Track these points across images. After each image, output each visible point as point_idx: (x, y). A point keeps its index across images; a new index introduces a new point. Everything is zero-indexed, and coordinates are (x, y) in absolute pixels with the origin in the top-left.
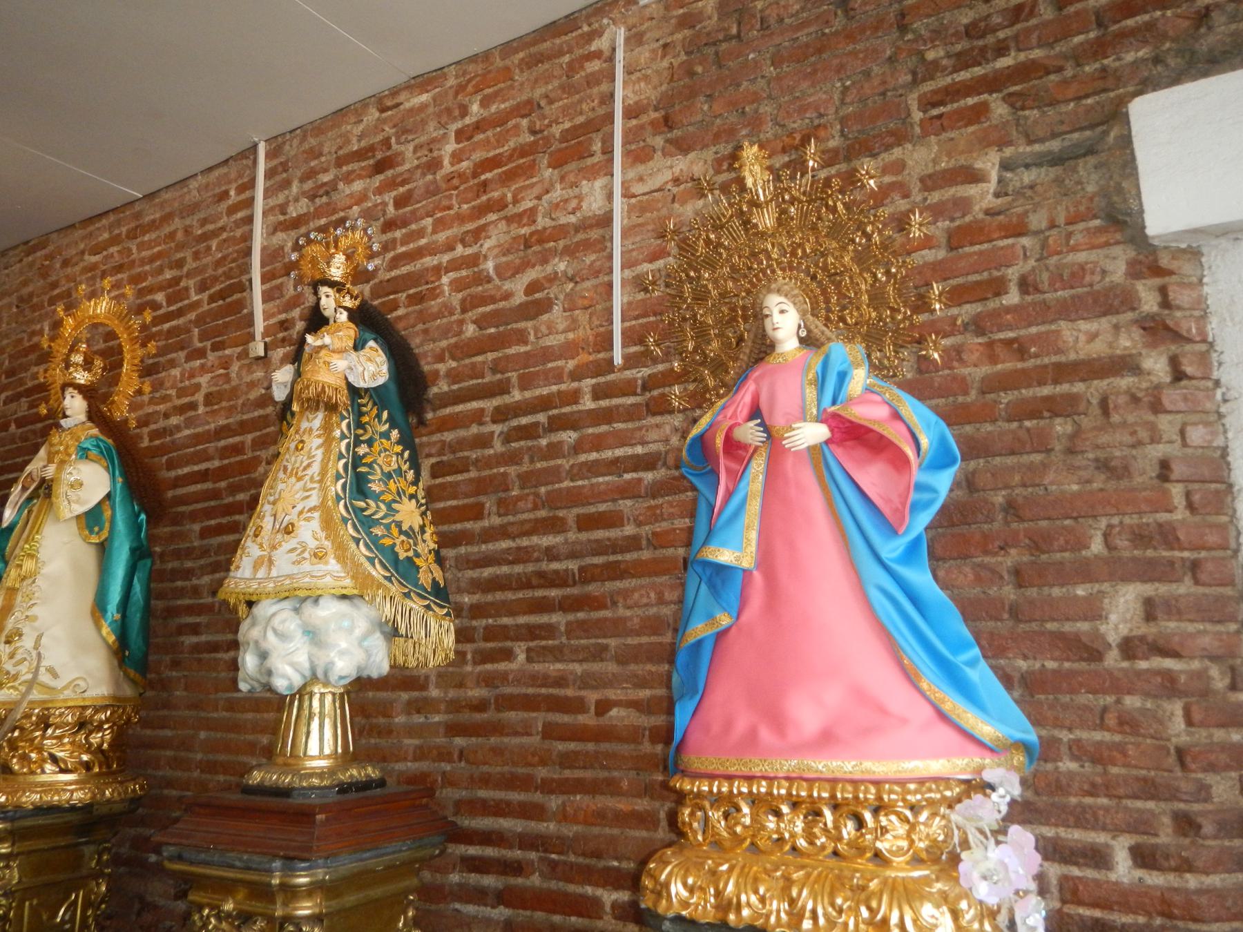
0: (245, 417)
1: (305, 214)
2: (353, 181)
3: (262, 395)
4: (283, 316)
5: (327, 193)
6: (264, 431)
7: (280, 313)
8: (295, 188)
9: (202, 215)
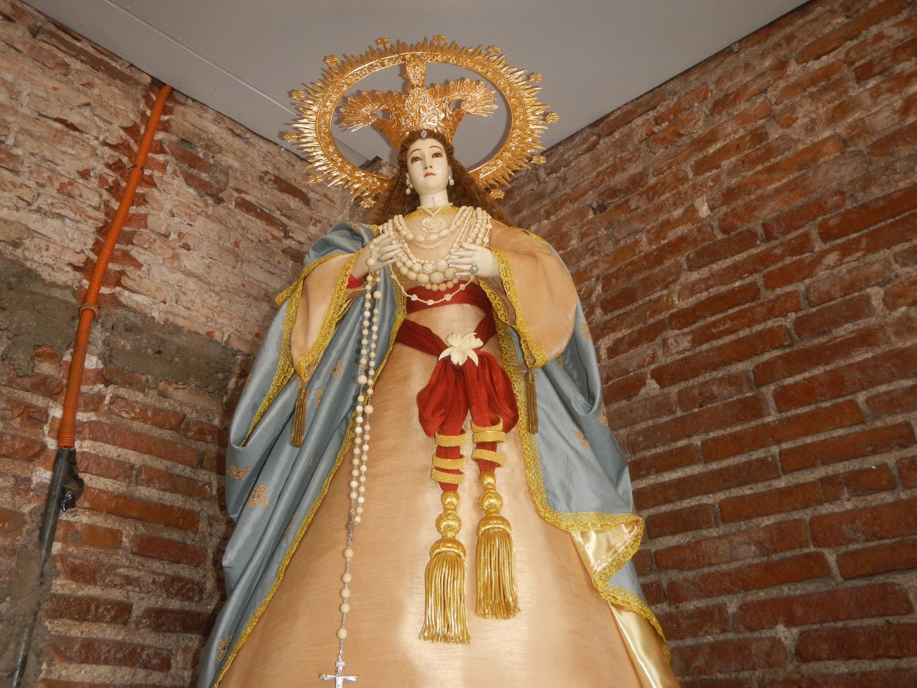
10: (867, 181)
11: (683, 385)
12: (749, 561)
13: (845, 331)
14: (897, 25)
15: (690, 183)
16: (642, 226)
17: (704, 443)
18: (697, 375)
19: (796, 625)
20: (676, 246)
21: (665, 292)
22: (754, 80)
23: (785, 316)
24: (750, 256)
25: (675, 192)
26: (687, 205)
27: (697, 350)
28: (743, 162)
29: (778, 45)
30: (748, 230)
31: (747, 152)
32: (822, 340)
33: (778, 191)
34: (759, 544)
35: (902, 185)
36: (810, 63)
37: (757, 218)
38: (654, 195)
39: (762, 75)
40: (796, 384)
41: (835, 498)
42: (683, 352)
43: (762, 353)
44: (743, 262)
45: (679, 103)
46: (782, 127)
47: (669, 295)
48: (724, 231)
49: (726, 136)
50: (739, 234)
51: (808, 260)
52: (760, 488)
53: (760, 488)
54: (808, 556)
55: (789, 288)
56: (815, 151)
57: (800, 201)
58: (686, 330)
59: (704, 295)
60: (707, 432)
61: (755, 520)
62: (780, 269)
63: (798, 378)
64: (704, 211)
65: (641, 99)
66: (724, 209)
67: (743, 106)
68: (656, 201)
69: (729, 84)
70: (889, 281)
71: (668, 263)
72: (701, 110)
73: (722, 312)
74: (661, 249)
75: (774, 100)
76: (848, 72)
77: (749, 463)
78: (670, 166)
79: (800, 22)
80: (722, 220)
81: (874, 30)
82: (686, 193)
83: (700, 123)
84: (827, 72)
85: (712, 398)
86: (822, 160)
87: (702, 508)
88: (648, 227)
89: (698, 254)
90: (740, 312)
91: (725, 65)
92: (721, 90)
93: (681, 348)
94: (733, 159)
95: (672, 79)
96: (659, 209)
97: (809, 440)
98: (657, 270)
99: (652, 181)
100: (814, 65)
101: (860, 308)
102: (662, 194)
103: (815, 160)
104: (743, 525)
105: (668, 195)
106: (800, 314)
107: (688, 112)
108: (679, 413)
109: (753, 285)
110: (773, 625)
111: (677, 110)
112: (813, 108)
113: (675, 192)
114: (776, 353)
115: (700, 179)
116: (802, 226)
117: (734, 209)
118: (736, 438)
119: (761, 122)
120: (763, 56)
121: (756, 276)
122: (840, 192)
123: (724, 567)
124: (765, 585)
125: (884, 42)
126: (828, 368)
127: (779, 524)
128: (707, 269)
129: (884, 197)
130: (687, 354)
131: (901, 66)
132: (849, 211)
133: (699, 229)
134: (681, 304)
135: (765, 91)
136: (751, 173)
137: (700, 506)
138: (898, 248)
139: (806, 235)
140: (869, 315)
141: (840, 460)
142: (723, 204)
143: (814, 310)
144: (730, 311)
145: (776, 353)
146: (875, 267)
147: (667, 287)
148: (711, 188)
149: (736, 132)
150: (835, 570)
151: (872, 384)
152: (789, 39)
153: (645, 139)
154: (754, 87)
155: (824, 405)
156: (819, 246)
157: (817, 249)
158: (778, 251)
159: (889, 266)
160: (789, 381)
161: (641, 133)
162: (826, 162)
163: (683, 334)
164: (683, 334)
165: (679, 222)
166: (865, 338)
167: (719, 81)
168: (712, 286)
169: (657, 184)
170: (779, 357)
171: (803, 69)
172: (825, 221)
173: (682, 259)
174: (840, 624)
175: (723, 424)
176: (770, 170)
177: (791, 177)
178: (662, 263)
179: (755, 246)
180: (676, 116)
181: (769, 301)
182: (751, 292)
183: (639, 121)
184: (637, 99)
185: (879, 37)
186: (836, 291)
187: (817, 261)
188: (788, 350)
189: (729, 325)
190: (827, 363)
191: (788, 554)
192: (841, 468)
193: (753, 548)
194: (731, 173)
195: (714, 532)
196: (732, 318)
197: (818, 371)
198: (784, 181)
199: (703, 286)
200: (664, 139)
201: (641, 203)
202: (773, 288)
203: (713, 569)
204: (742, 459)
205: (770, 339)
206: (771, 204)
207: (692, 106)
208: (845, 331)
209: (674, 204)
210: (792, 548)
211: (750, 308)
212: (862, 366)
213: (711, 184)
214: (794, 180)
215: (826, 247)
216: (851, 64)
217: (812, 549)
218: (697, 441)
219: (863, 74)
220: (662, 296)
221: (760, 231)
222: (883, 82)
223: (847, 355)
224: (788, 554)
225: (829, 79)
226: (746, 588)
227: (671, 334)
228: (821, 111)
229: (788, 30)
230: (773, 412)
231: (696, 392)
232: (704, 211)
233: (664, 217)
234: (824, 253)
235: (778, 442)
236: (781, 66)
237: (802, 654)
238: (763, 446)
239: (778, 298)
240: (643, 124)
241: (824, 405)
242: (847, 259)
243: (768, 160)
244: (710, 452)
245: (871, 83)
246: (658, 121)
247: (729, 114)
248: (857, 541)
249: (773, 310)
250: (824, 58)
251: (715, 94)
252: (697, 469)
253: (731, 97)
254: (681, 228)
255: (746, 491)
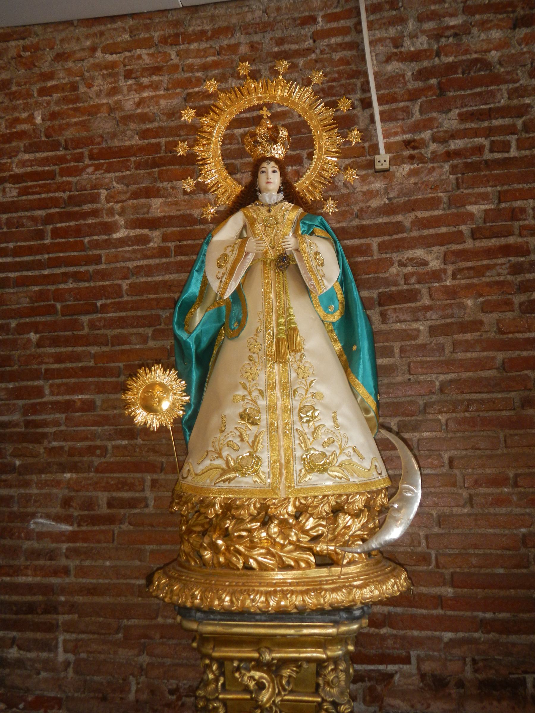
0: (365, 222)
1: (425, 50)
2: (489, 29)
3: (385, 204)
4: (408, 136)
5: (456, 35)
6: (395, 237)
7: (404, 132)
8: (411, 25)
9: (278, 34)
10: (114, 135)
11: (9, 215)
12: (25, 305)
13: (87, 207)
14: (148, 54)
15: (35, 99)
16: (3, 115)
17: (15, 247)
18: (17, 212)
19: (39, 333)
20: (21, 135)
21: (9, 161)
22: (79, 50)
23: (64, 191)
24: (56, 155)
25: (25, 101)
26: (30, 112)
27: (20, 198)
28: (64, 99)
29: (95, 35)
30: (58, 140)
31: (67, 94)
32: (77, 209)
33: (76, 124)
34: (31, 298)
35: (127, 143)
36: (107, 56)
37: (63, 135)
38: (14, 98)
39: (83, 50)
40: (62, 227)
41: (65, 282)
42: (13, 197)
43: (51, 208)
44: (52, 157)
45: (38, 43)
46: (86, 87)
47: (11, 163)
48: (47, 136)
49: (59, 79)
50: (53, 140)
51: (80, 167)
52: (36, 273)
53: (36, 273)
54: (50, 305)
55: (70, 179)
56: (98, 108)
57: (84, 134)
58: (17, 186)
59: (29, 169)
60: (17, 242)
61: (30, 287)
62: (67, 167)
63: (63, 224)
64: (38, 120)
65: (17, 29)
66: (49, 123)
67: (70, 64)
68: (14, 102)
69: (67, 45)
70: (110, 189)
71: (14, 144)
72: (49, 55)
73: (36, 181)
74: (12, 134)
75: (86, 68)
76: (121, 70)
77: (33, 261)
78: (25, 84)
79: (109, 26)
80: (47, 129)
81: (138, 52)
82: (31, 105)
83: (47, 63)
84: (113, 65)
85: (23, 225)
86: (99, 115)
87: (8, 278)
88: (7, 117)
89: (30, 145)
90: (45, 184)
91: (67, 31)
92: (62, 48)
93: (12, 195)
94: (59, 95)
95: (38, 24)
96: (15, 108)
97: (61, 255)
98: (7, 146)
99: (14, 88)
100: (110, 58)
101: (95, 199)
102: (19, 100)
103: (96, 113)
104: (25, 289)
105: (21, 102)
106: (71, 193)
107: (41, 52)
108: (5, 230)
109: (53, 171)
110: (29, 333)
111: (36, 48)
112: (102, 84)
113: (25, 101)
114: (57, 210)
115: (40, 99)
116: (82, 148)
117: (53, 126)
118: (30, 247)
119: (78, 79)
120: (87, 37)
121: (56, 168)
122: (101, 136)
123: (13, 307)
124: (29, 316)
125: (141, 61)
126: (77, 223)
127: (40, 291)
128: (33, 155)
129: (118, 147)
130: (15, 199)
131: (143, 79)
132: (103, 148)
133: (34, 130)
134: (17, 170)
135: (83, 60)
136: (66, 107)
137: (7, 277)
138: (117, 174)
139: (82, 153)
140: (98, 203)
141: (71, 266)
142: (49, 120)
143: (77, 193)
144: (41, 182)
145: (57, 210)
146: (107, 181)
147: (10, 158)
148: (45, 107)
149: (64, 79)
150: (60, 312)
151: (92, 235)
152: (102, 34)
153: (15, 58)
154: (78, 55)
155: (71, 240)
156: (87, 161)
157: (86, 162)
158: (69, 157)
159: (111, 182)
160: (59, 225)
161: (13, 53)
162: (100, 117)
163: (15, 188)
164: (15, 188)
165: (25, 121)
166: (95, 213)
167: (62, 41)
168: (34, 166)
169: (16, 92)
170: (58, 212)
171: (104, 57)
172: (92, 149)
173: (22, 145)
174: (56, 334)
175: (25, 240)
176: (76, 110)
177: (84, 118)
178: (10, 143)
179: (59, 150)
180: (35, 52)
181: (59, 183)
182: (51, 175)
183: (13, 43)
184: (15, 27)
185: (140, 57)
186: (88, 187)
187: (84, 169)
188: (63, 210)
189: (38, 189)
190: (77, 221)
191: (42, 304)
192: (71, 269)
193: (28, 299)
194: (57, 103)
195: (11, 290)
196: (40, 186)
197: (72, 223)
198: (81, 119)
199: (29, 164)
200: (25, 64)
201: (5, 101)
202: (62, 176)
203: (8, 307)
204: (31, 258)
205: (55, 202)
206: (72, 130)
207: (45, 49)
208: (87, 207)
209: (24, 109)
210: (44, 301)
211: (50, 183)
212: (89, 226)
213: (45, 105)
214: (86, 120)
215: (90, 163)
216: (125, 66)
217: (52, 302)
218: (11, 245)
219: (128, 75)
220: (7, 162)
221: (63, 143)
222: (134, 84)
223: (85, 219)
224: (42, 304)
225: (113, 70)
226: (21, 317)
227: (8, 185)
228: (105, 87)
229: (103, 28)
230: (49, 238)
231: (15, 220)
232: (38, 120)
233: (16, 114)
234: (88, 166)
235: (48, 253)
236: (93, 49)
237: (39, 345)
238: (41, 254)
239: (63, 182)
240: (15, 47)
241: (71, 240)
242: (97, 172)
243: (75, 103)
244: (16, 252)
245: (130, 82)
246: (25, 49)
247: (63, 66)
248: (70, 301)
249: (61, 188)
250: (114, 56)
251: (58, 48)
252: (9, 260)
253: (66, 55)
254: (25, 125)
255: (30, 273)
